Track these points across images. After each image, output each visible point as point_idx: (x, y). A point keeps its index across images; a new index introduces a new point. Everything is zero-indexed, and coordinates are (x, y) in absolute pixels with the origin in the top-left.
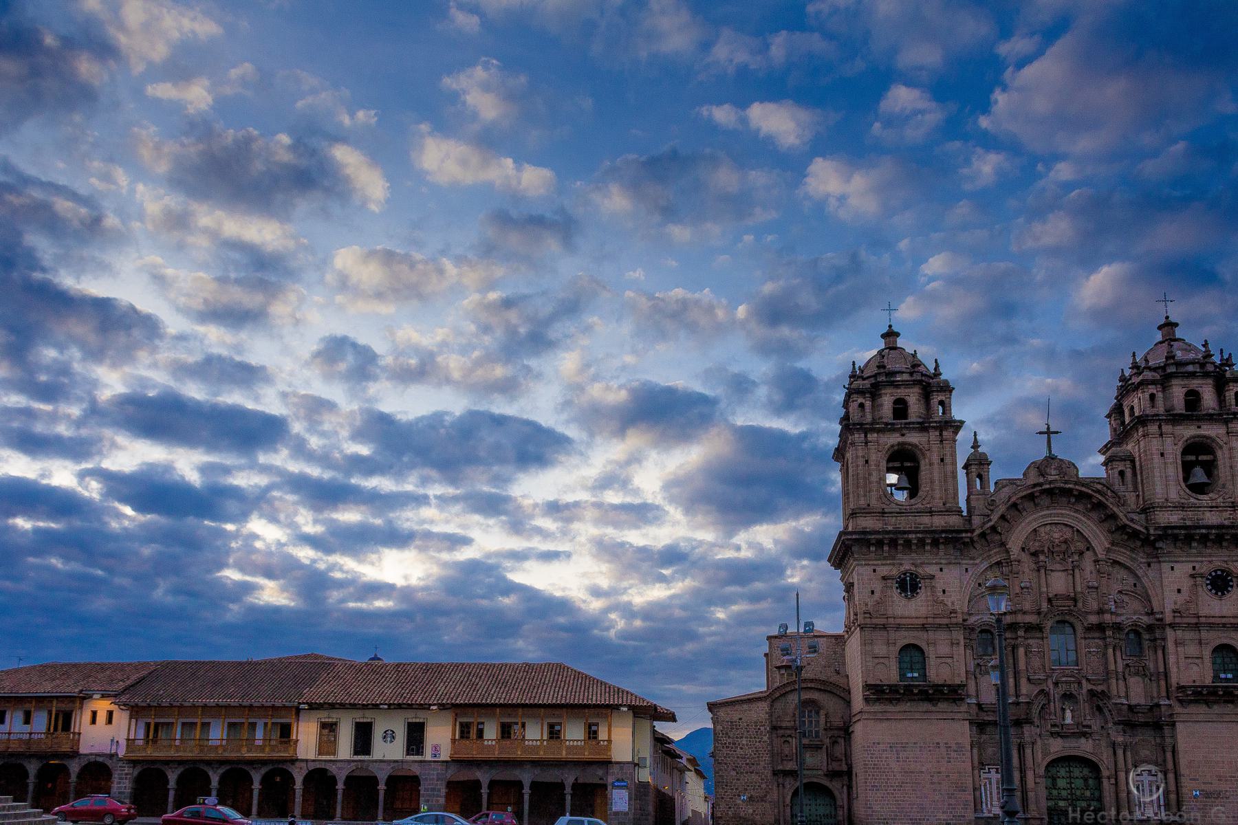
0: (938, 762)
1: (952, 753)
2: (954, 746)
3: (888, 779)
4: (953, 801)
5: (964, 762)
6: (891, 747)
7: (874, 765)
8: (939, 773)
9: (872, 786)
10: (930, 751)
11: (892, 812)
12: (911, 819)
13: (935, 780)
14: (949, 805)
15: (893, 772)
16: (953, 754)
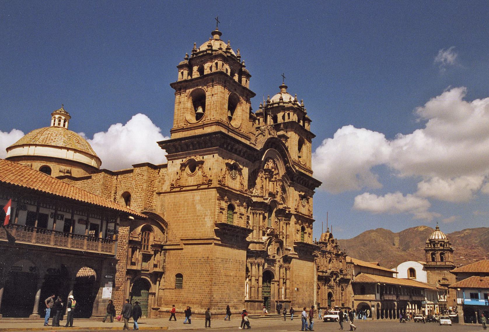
0: (236, 270)
1: (241, 266)
2: (241, 262)
3: (220, 279)
4: (239, 292)
5: (244, 271)
6: (222, 261)
7: (216, 271)
8: (236, 276)
9: (215, 283)
10: (234, 264)
11: (220, 298)
12: (226, 302)
13: (235, 281)
14: (238, 294)
15: (222, 275)
16: (241, 267)
